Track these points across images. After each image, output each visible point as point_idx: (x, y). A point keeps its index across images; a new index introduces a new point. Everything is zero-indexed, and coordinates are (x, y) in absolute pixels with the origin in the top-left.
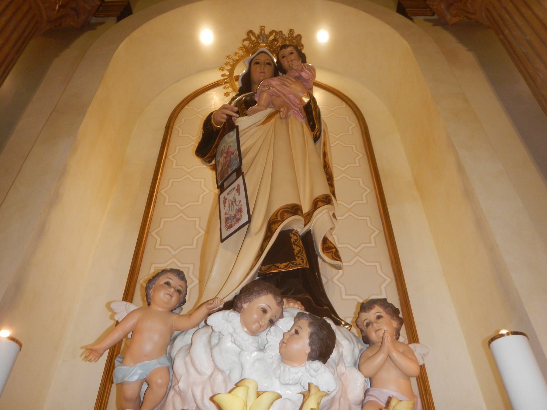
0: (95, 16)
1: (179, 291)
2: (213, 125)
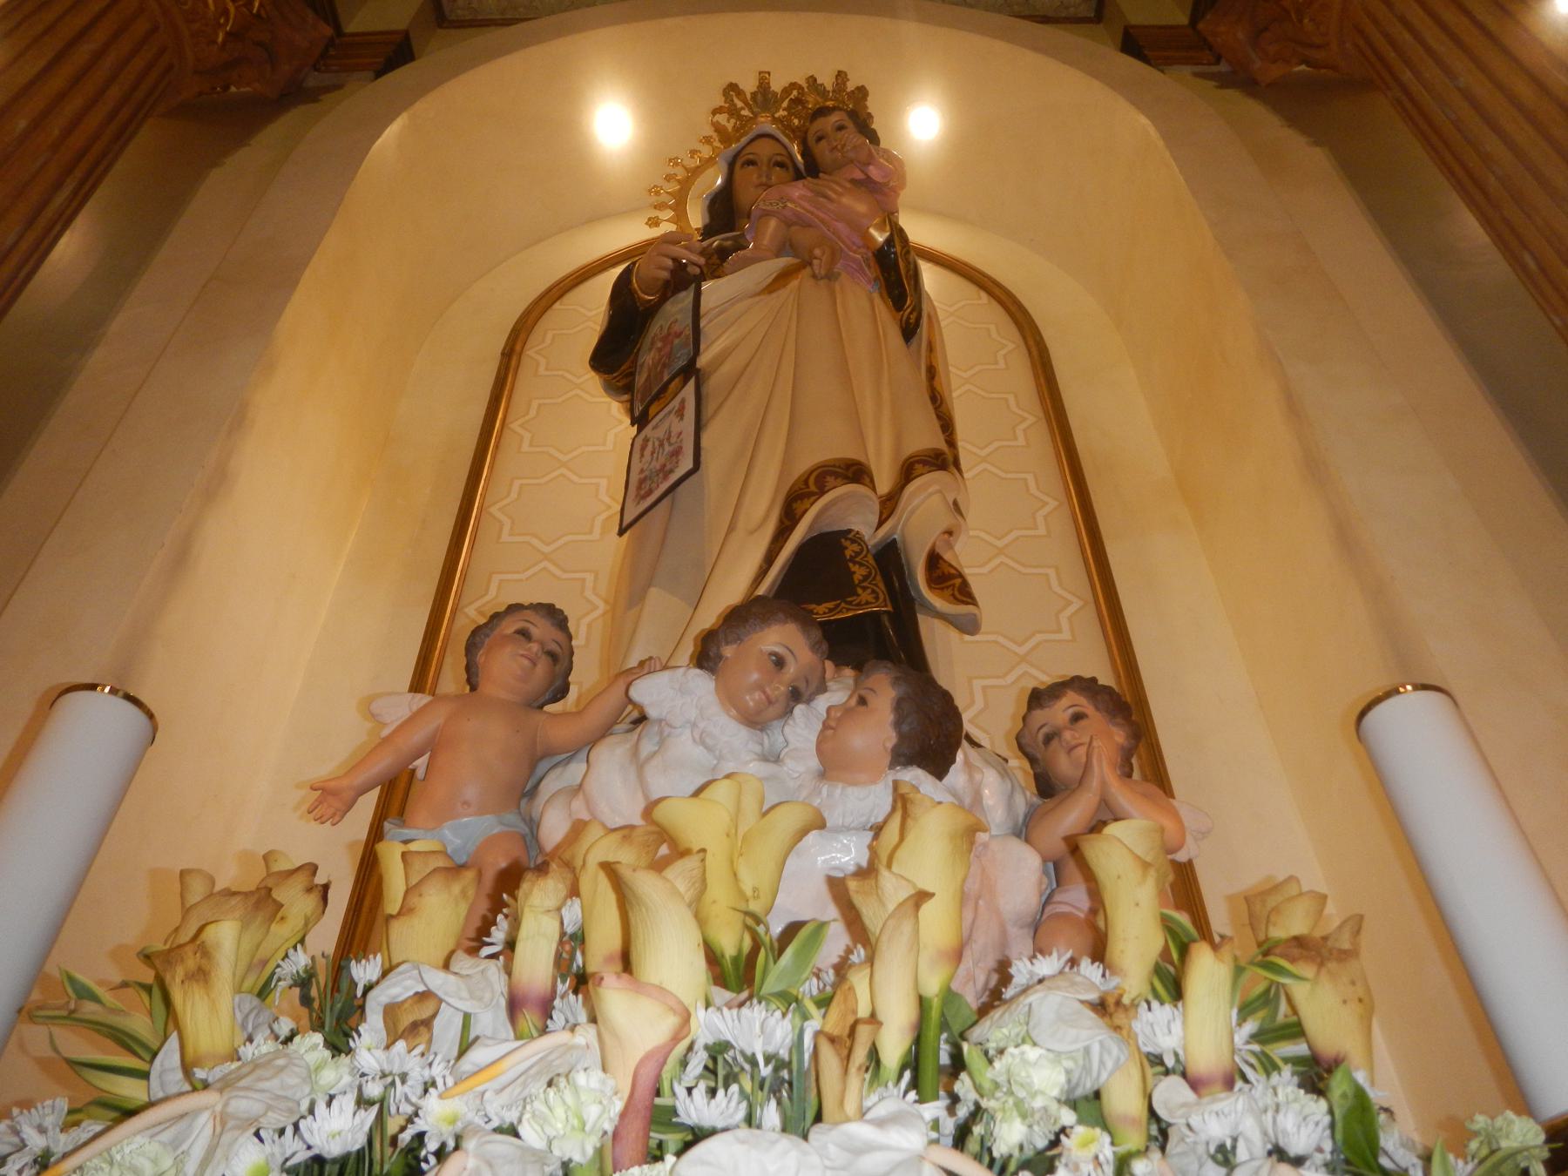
0: (316, 70)
1: (553, 656)
2: (636, 293)
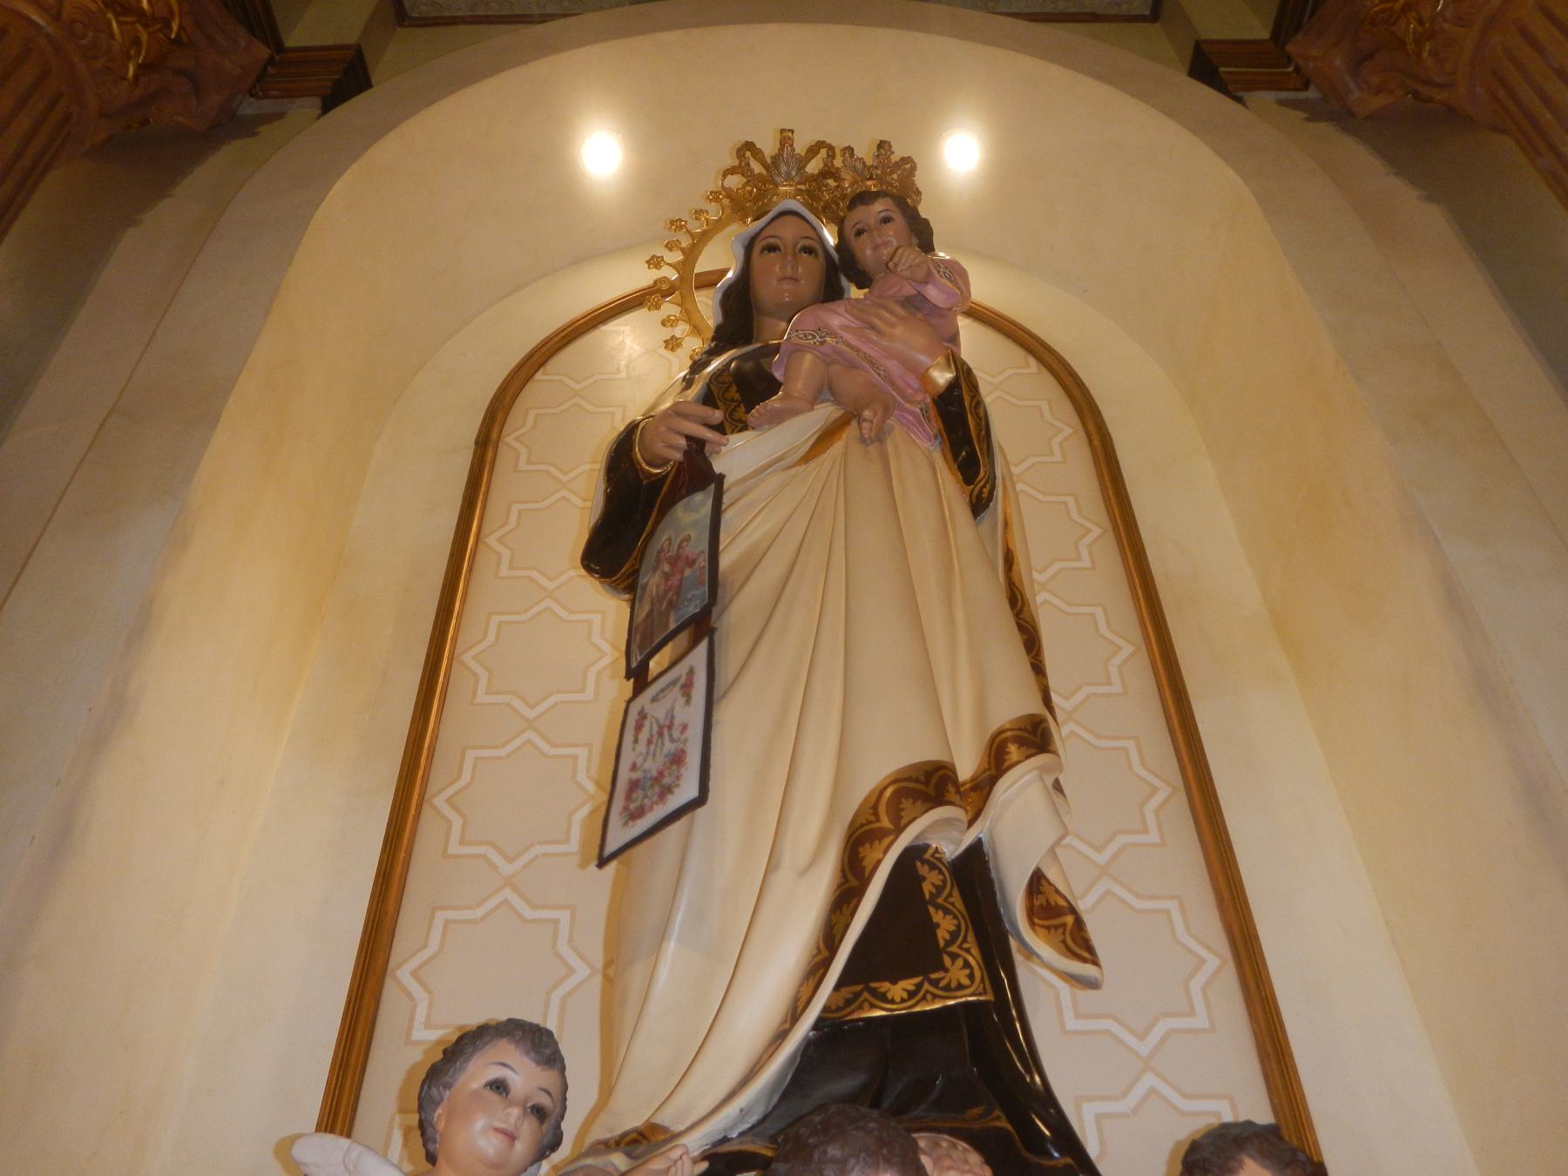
0: (252, 95)
1: (539, 1112)
2: (640, 465)
